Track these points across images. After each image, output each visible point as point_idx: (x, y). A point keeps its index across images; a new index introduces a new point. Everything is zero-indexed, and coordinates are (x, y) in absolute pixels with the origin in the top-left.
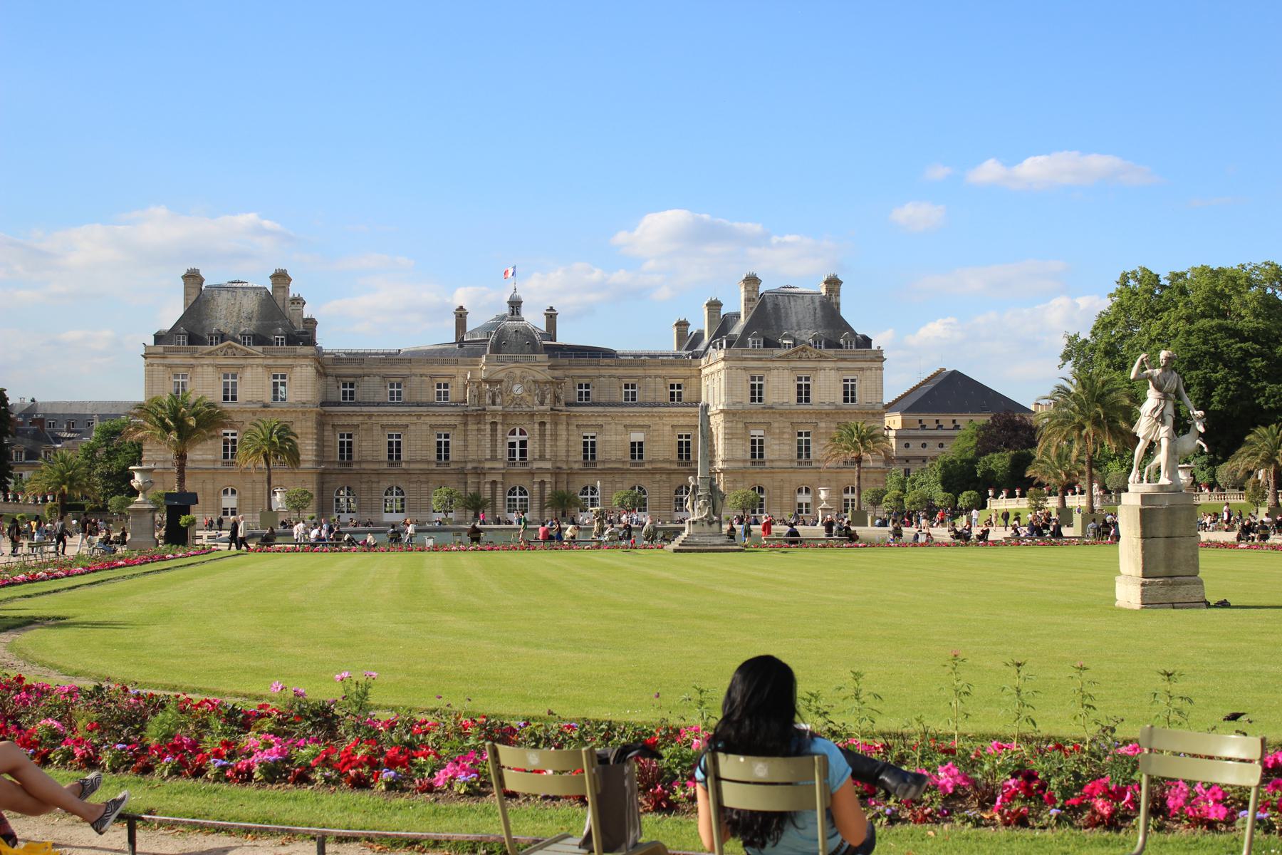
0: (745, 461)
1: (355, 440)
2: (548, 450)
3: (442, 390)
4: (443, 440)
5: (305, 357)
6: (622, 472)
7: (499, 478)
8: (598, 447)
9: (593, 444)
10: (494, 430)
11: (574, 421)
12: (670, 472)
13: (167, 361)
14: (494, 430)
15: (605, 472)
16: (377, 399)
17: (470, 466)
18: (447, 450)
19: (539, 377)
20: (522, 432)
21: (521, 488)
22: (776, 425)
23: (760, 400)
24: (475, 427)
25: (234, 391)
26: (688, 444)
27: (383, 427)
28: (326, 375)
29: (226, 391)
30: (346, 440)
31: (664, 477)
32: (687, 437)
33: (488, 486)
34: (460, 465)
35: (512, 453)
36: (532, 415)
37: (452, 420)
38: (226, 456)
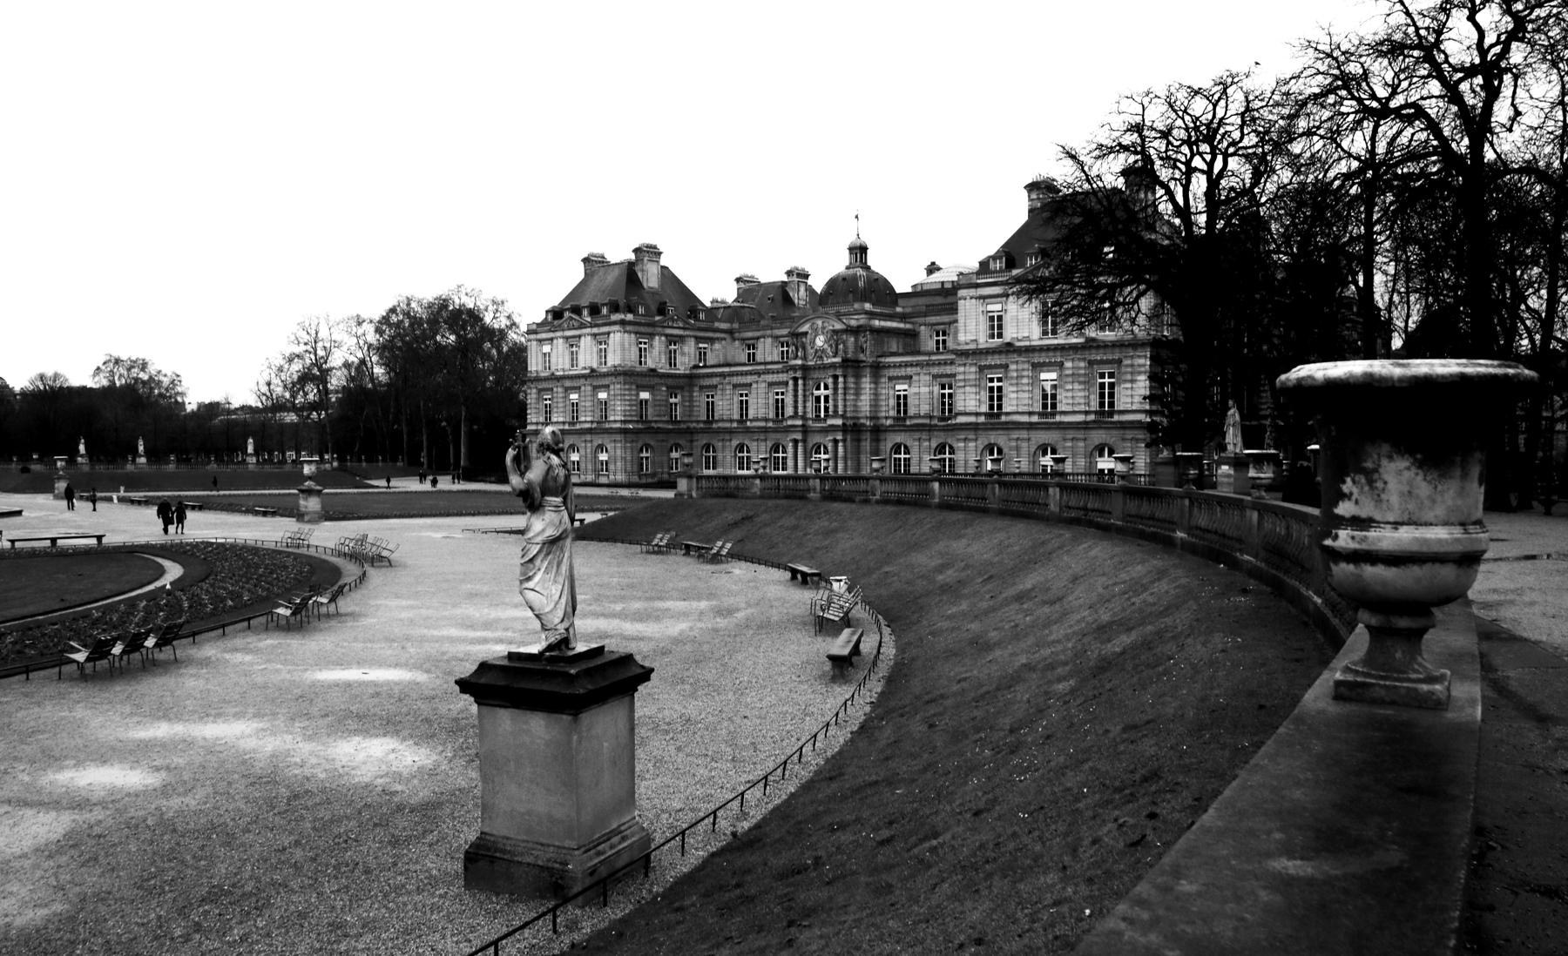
0: (977, 414)
2: (840, 403)
5: (614, 323)
6: (930, 429)
7: (799, 436)
9: (905, 397)
10: (796, 385)
13: (540, 336)
14: (796, 385)
16: (769, 359)
19: (838, 326)
20: (826, 388)
22: (1013, 367)
23: (1000, 335)
27: (735, 386)
28: (734, 339)
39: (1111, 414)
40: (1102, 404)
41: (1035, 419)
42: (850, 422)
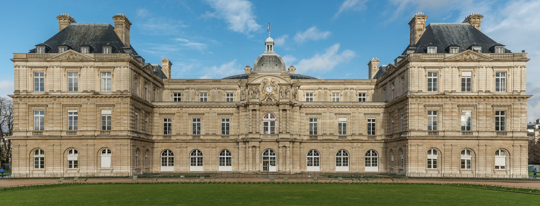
1: (173, 122)
3: (230, 97)
4: (225, 122)
7: (257, 144)
8: (319, 127)
9: (315, 124)
11: (303, 110)
12: (363, 142)
15: (323, 141)
17: (241, 137)
18: (228, 129)
19: (282, 82)
21: (271, 151)
24: (244, 114)
25: (76, 84)
26: (374, 125)
27: (190, 114)
29: (70, 84)
30: (167, 122)
31: (359, 144)
32: (374, 120)
33: (250, 149)
34: (237, 137)
35: (266, 129)
36: (278, 105)
37: (231, 110)
38: (70, 128)
39: (506, 133)
40: (497, 128)
41: (460, 134)
42: (292, 137)
